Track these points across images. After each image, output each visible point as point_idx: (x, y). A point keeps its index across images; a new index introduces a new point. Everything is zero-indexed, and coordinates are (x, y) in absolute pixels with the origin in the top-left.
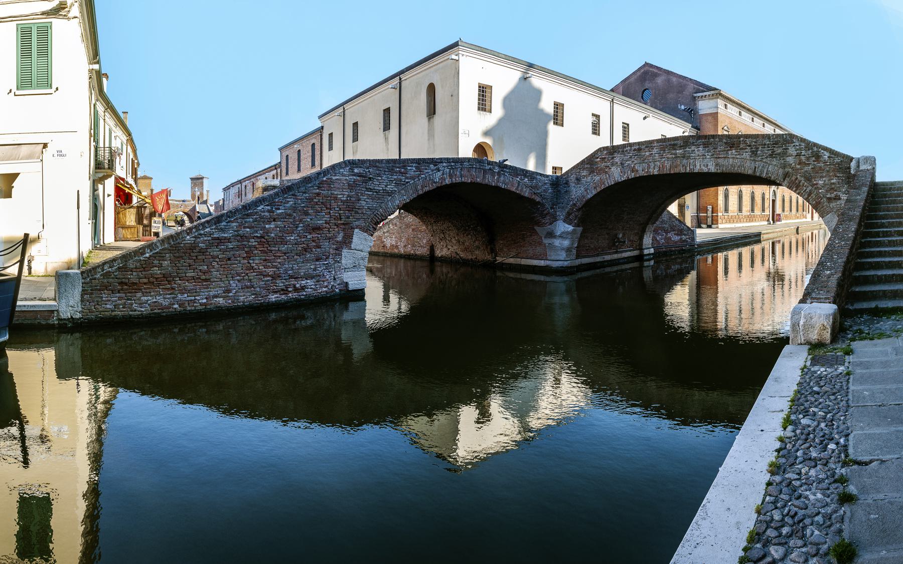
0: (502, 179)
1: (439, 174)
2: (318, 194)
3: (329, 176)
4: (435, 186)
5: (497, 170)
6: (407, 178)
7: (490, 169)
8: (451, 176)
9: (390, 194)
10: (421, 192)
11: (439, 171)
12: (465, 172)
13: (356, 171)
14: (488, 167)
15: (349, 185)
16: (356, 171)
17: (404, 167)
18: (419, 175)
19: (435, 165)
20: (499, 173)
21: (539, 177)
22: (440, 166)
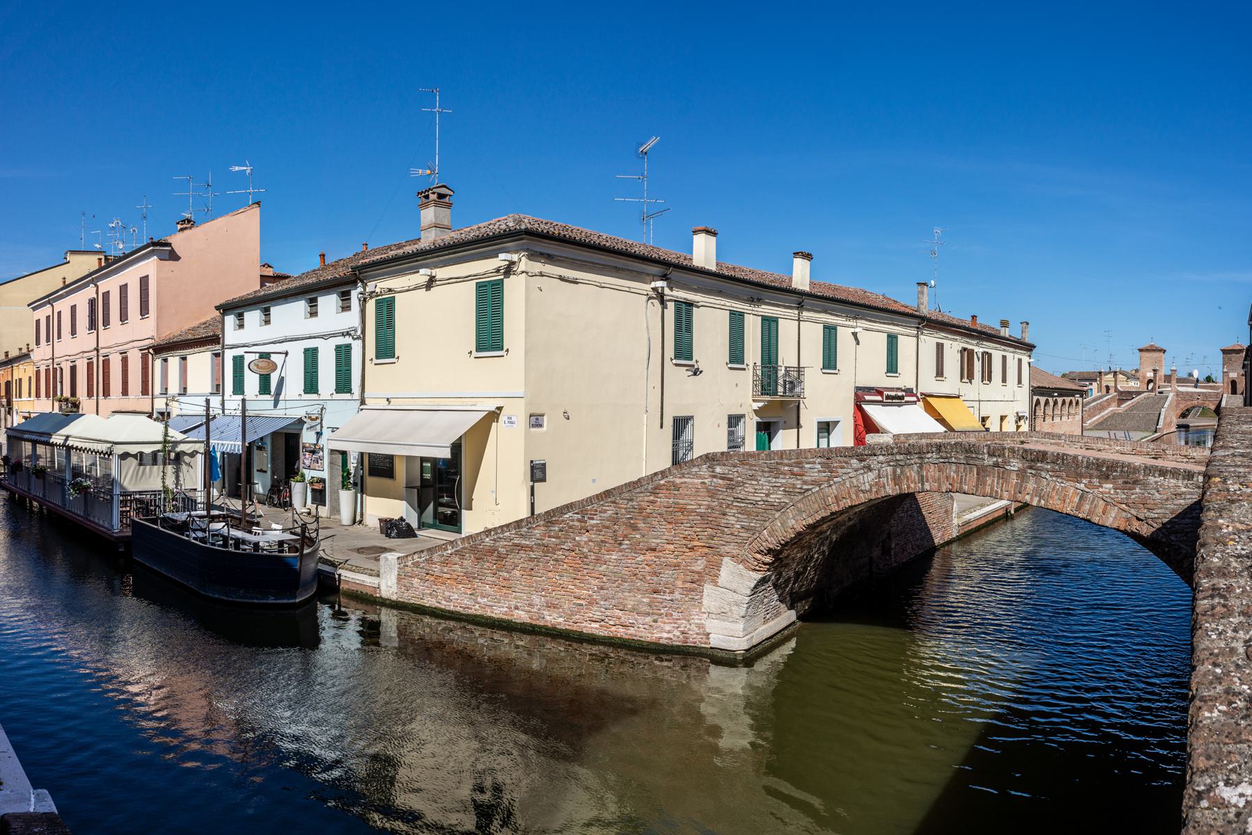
0: (1031, 485)
1: (871, 476)
2: (653, 502)
3: (671, 478)
4: (863, 498)
5: (1015, 465)
6: (805, 483)
7: (996, 465)
8: (896, 480)
9: (780, 507)
10: (835, 508)
11: (869, 469)
12: (932, 472)
13: (718, 470)
14: (988, 461)
15: (708, 491)
16: (718, 470)
17: (799, 464)
18: (830, 479)
19: (861, 461)
20: (1022, 474)
21: (1151, 479)
22: (873, 462)
